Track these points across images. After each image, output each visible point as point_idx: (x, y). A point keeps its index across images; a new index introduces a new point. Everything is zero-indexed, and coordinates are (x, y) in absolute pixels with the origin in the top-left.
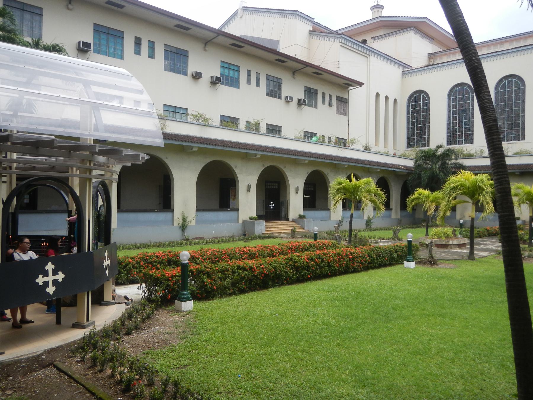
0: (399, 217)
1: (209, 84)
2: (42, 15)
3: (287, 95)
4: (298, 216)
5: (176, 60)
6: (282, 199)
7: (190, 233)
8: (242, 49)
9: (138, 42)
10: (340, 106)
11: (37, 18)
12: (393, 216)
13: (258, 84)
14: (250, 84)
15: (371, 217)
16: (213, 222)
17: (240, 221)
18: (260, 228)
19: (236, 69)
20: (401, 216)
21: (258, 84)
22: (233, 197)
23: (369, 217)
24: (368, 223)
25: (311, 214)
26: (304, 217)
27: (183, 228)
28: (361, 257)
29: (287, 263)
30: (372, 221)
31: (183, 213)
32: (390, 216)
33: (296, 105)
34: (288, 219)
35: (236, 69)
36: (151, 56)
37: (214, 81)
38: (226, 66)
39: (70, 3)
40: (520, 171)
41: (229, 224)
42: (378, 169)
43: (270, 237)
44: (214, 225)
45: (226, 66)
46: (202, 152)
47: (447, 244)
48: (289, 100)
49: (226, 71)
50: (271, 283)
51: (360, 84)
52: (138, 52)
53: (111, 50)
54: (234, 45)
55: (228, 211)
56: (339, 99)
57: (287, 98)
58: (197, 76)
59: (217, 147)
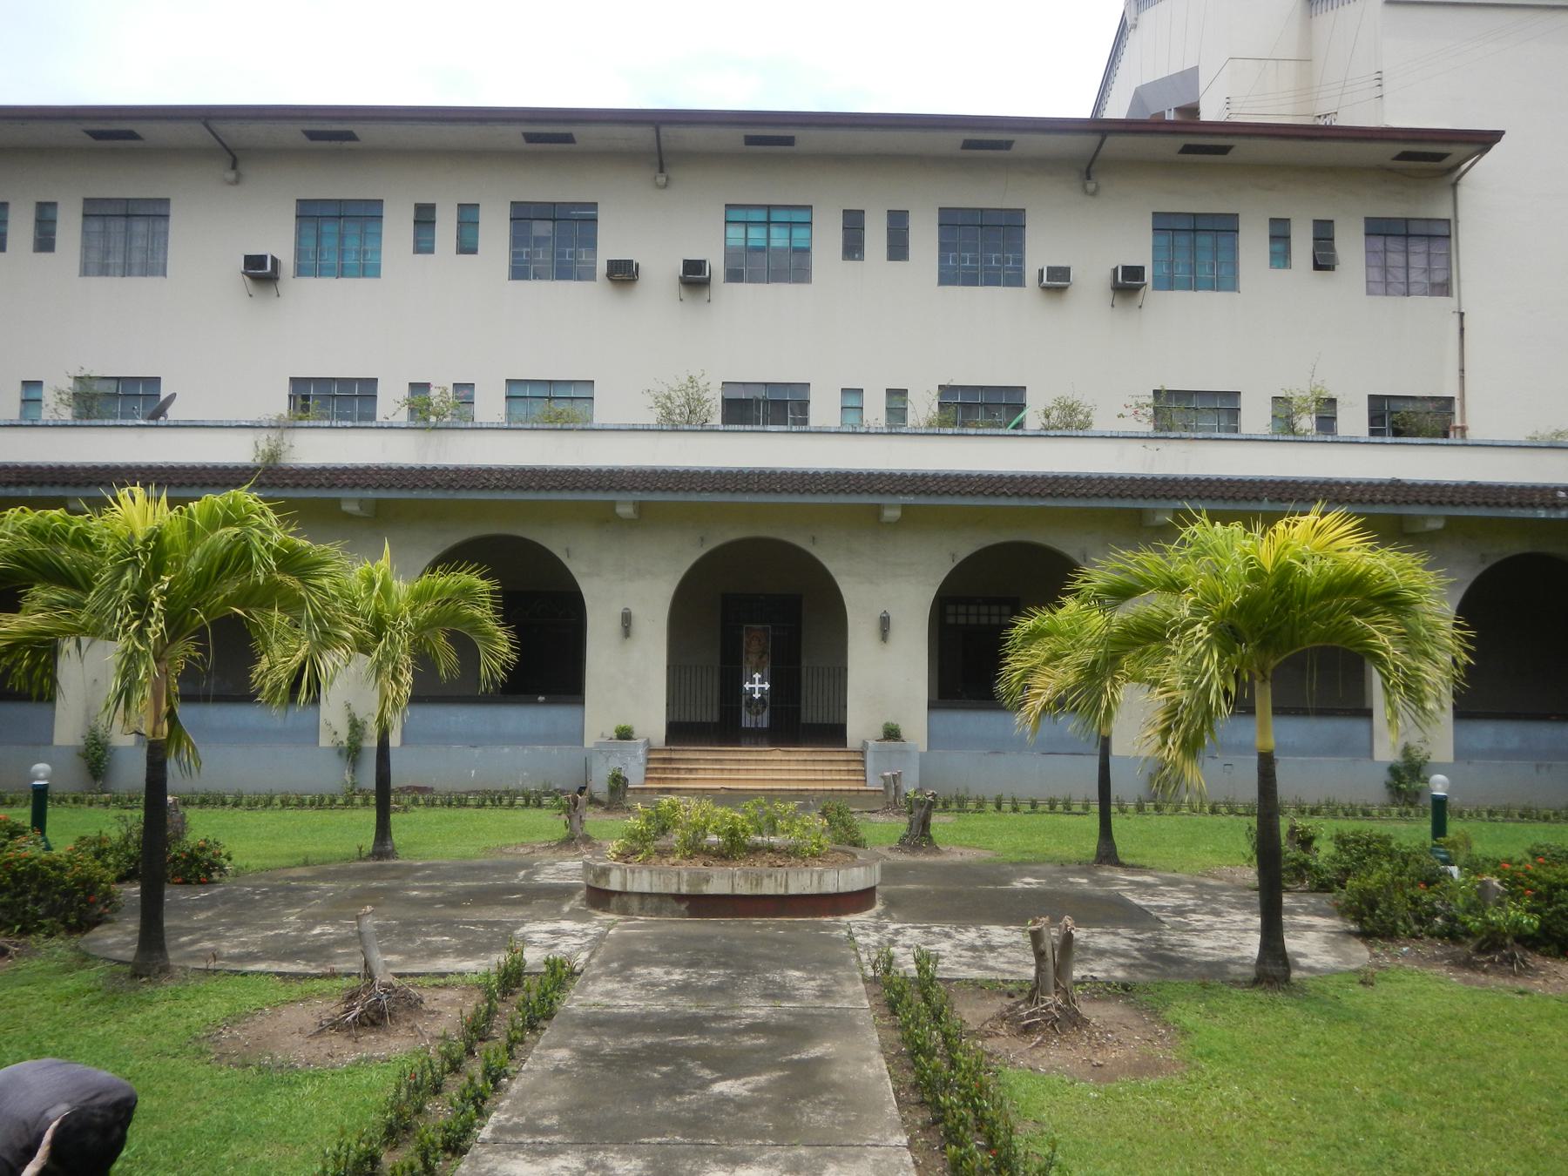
2: (166, 217)
9: (424, 218)
10: (1396, 259)
13: (898, 248)
14: (861, 258)
16: (474, 740)
21: (898, 248)
22: (754, 658)
23: (1406, 750)
31: (348, 706)
33: (1111, 293)
36: (467, 247)
38: (760, 216)
42: (1424, 518)
44: (477, 751)
45: (760, 216)
47: (602, 885)
48: (1057, 281)
49: (757, 235)
51: (1485, 140)
52: (424, 244)
53: (351, 260)
55: (537, 703)
56: (1377, 229)
58: (623, 274)
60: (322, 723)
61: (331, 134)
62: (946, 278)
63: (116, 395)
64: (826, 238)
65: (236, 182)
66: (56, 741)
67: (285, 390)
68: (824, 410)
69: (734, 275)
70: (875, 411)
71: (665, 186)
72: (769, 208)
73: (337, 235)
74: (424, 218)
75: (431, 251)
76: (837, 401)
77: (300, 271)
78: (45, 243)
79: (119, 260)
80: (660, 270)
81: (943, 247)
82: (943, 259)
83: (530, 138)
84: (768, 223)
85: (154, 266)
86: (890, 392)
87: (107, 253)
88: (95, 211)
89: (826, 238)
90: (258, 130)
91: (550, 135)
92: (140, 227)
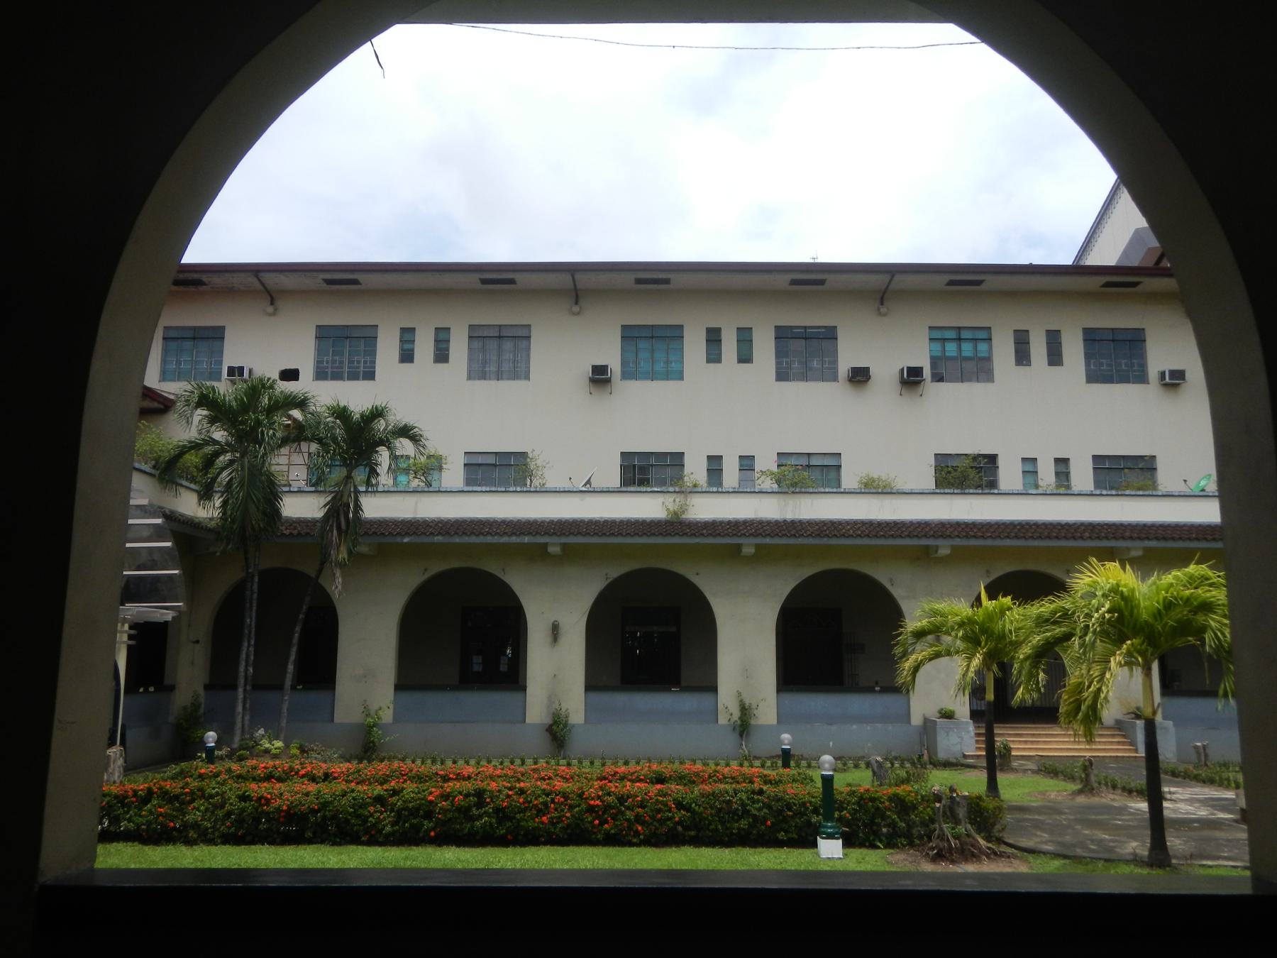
1: (897, 386)
2: (529, 337)
3: (1162, 369)
5: (804, 353)
7: (760, 745)
8: (983, 287)
9: (714, 337)
11: (525, 343)
13: (1055, 357)
14: (1029, 364)
16: (830, 720)
17: (916, 720)
18: (954, 739)
19: (983, 335)
21: (1055, 357)
27: (744, 726)
28: (642, 806)
29: (379, 800)
31: (739, 694)
35: (983, 335)
36: (745, 357)
37: (911, 379)
38: (952, 334)
39: (576, 303)
41: (879, 725)
44: (834, 728)
45: (952, 334)
46: (764, 556)
49: (951, 349)
50: (309, 834)
53: (659, 367)
54: (951, 283)
55: (874, 691)
57: (1163, 374)
58: (860, 376)
59: (800, 541)
60: (720, 706)
61: (653, 280)
62: (1092, 378)
63: (495, 465)
64: (1003, 351)
65: (578, 314)
66: (528, 720)
67: (618, 461)
68: (1009, 475)
69: (938, 378)
70: (1047, 475)
71: (884, 315)
72: (959, 328)
73: (651, 350)
74: (714, 337)
75: (719, 361)
76: (1019, 467)
77: (626, 375)
78: (442, 356)
79: (493, 368)
80: (885, 370)
81: (1088, 356)
82: (1087, 364)
83: (794, 282)
84: (959, 339)
85: (520, 372)
86: (1057, 461)
87: (485, 363)
88: (477, 335)
89: (1003, 351)
90: (603, 279)
91: (810, 281)
92: (508, 345)
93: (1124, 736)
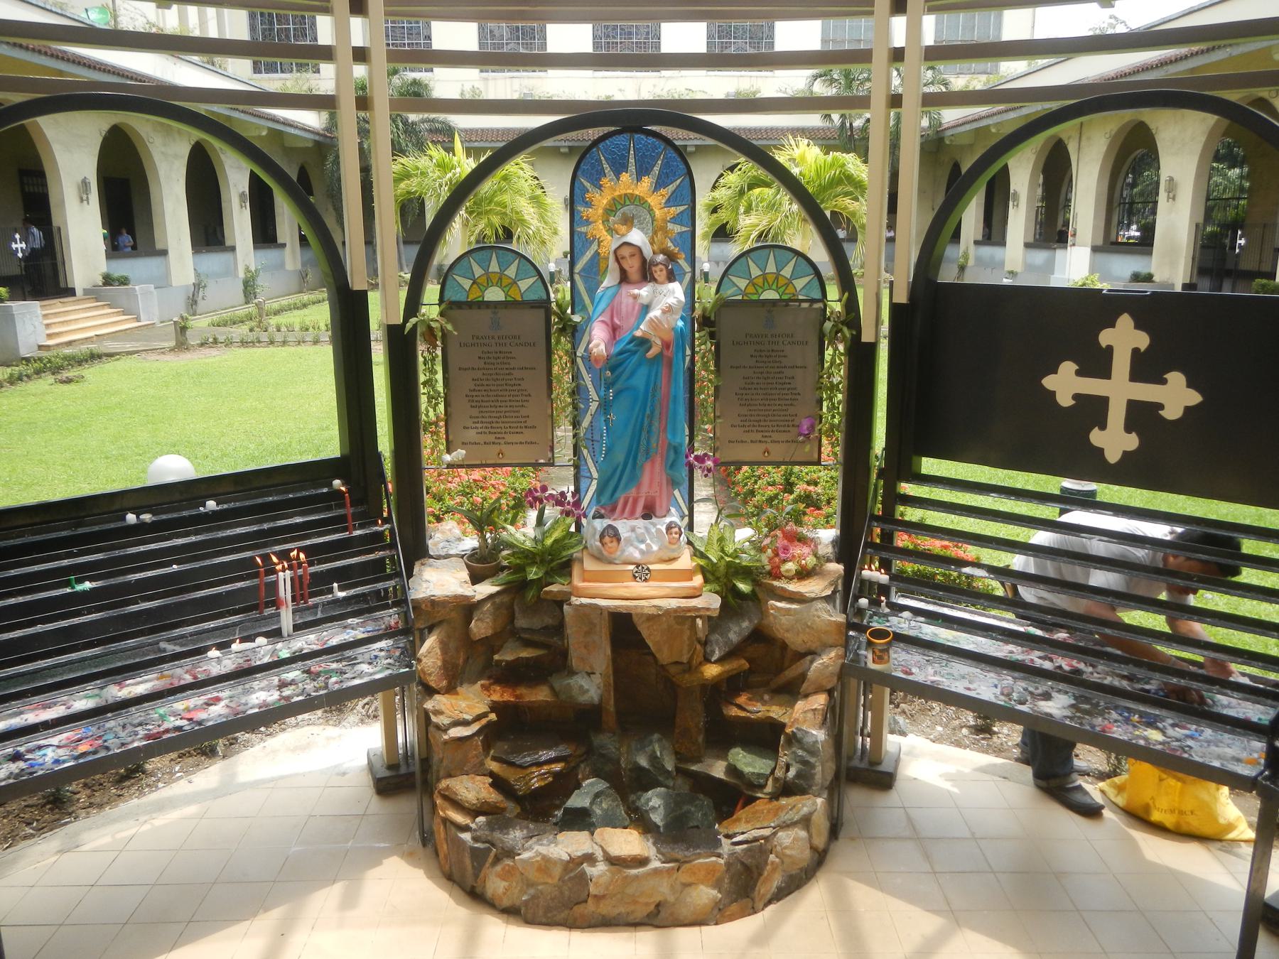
0: (299, 267)
4: (100, 281)
6: (56, 221)
12: (289, 266)
15: (253, 268)
20: (304, 264)
23: (247, 270)
24: (249, 289)
25: (123, 267)
26: (124, 281)
30: (259, 281)
32: (282, 265)
34: (71, 292)
40: (567, 144)
42: (259, 127)
43: (94, 357)
93: (110, 306)
